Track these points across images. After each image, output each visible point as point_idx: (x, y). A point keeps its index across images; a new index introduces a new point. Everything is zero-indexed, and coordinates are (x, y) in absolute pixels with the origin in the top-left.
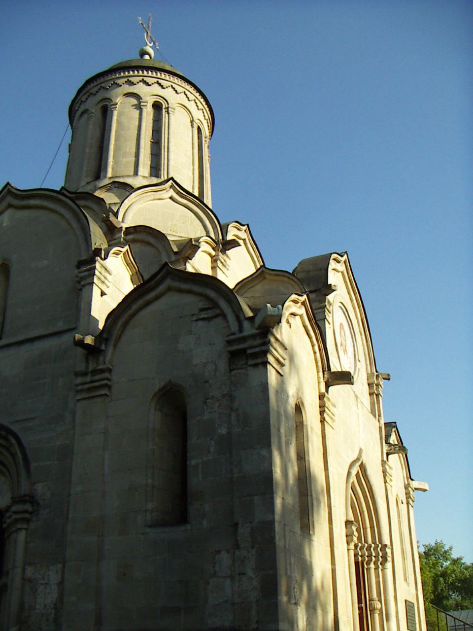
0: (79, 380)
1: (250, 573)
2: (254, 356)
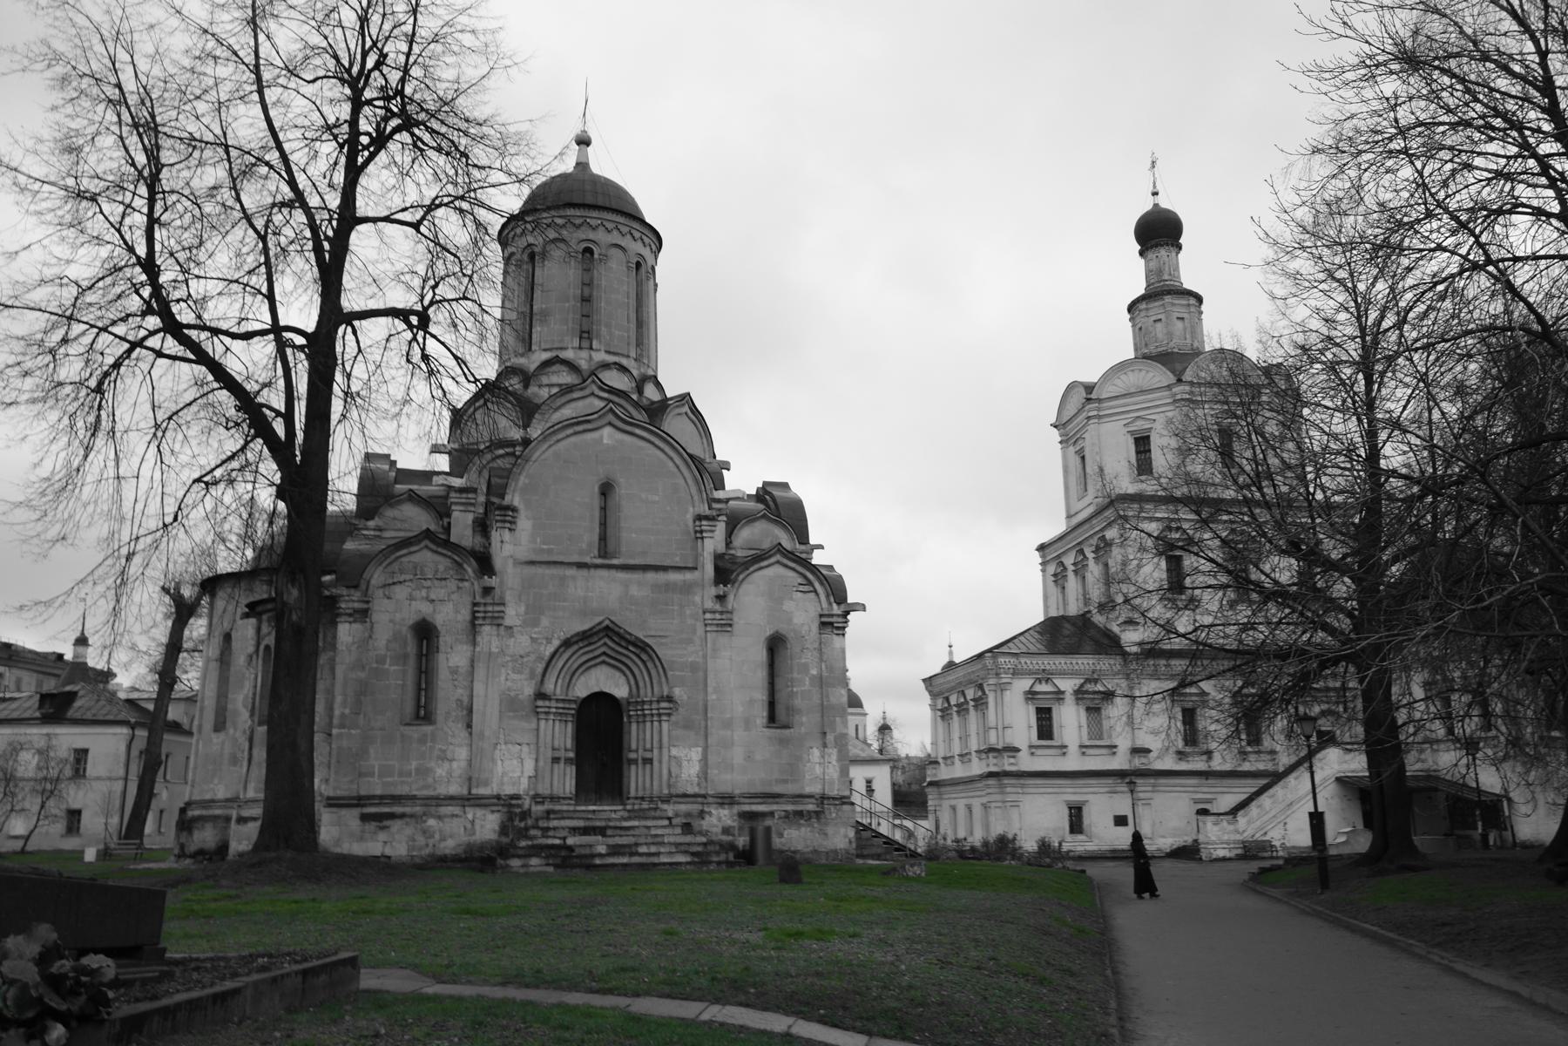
0: (708, 616)
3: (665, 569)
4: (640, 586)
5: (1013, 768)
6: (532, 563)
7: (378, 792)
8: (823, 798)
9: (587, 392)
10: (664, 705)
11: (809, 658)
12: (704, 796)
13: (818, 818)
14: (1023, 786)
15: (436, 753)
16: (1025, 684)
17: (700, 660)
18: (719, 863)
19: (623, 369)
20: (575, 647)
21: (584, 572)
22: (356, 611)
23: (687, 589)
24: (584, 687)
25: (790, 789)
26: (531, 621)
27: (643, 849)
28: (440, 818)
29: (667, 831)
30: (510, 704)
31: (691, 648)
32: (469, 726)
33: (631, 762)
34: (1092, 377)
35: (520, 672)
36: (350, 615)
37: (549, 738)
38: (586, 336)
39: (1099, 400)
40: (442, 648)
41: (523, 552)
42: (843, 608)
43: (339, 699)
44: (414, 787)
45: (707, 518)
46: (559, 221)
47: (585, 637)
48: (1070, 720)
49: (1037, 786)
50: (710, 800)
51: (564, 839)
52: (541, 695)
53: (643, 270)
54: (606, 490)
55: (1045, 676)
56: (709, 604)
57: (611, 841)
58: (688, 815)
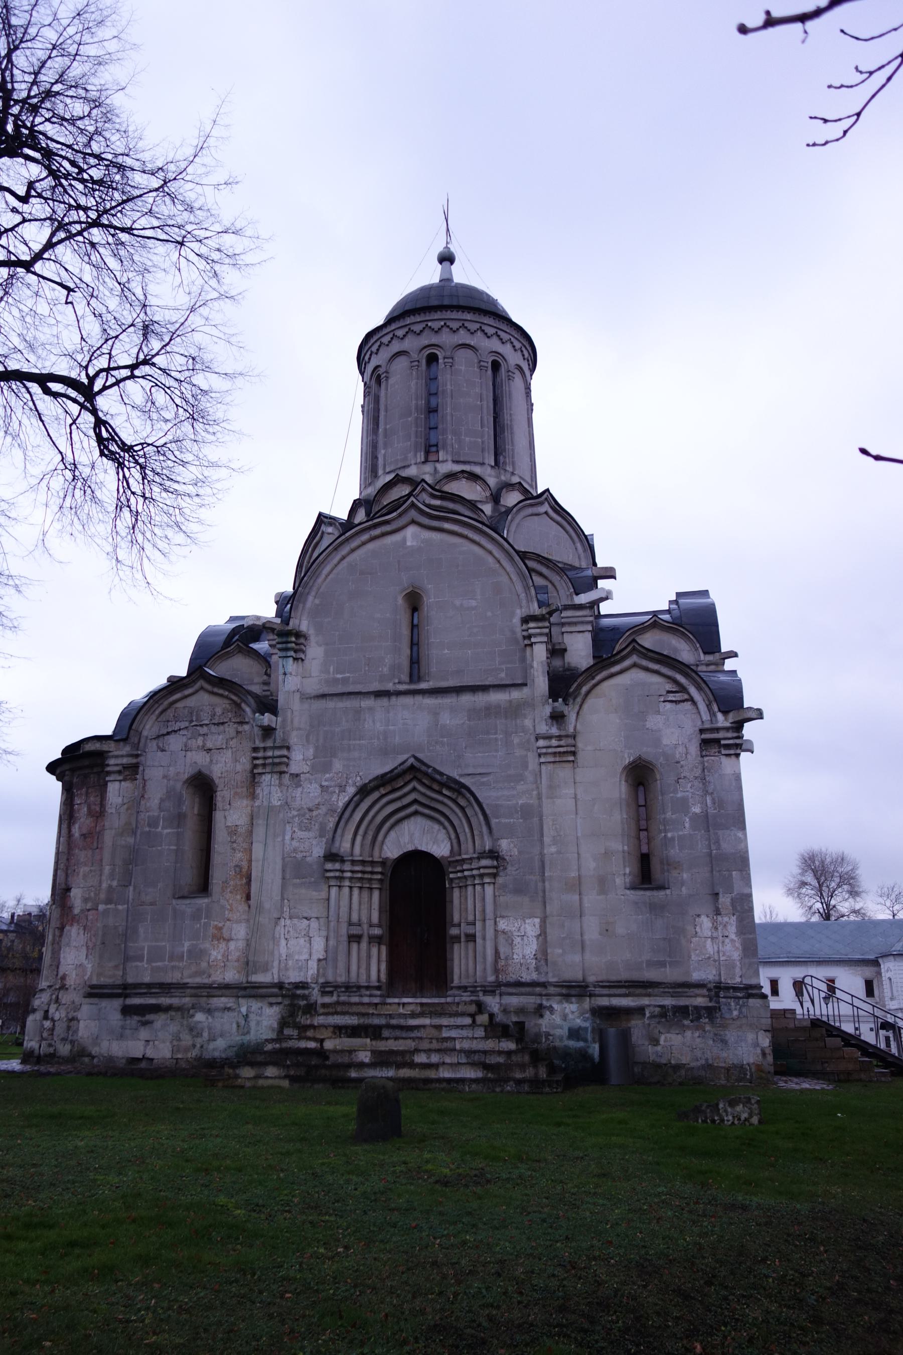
0: (541, 743)
1: (733, 936)
2: (727, 746)
3: (484, 688)
4: (452, 713)
6: (323, 696)
7: (147, 980)
8: (718, 989)
11: (688, 790)
12: (544, 985)
13: (711, 1018)
15: (211, 930)
18: (519, 1082)
19: (474, 477)
20: (376, 795)
21: (384, 701)
22: (126, 767)
23: (514, 711)
24: (394, 846)
25: (670, 975)
26: (321, 765)
27: (421, 1058)
28: (209, 1011)
29: (464, 1033)
30: (294, 869)
31: (521, 787)
32: (248, 897)
35: (308, 829)
36: (119, 772)
37: (344, 910)
38: (430, 450)
41: (313, 686)
42: (732, 717)
44: (186, 973)
46: (400, 333)
47: (385, 781)
51: (322, 1041)
52: (331, 856)
53: (503, 370)
54: (414, 601)
56: (543, 728)
57: (382, 1046)
58: (521, 1011)
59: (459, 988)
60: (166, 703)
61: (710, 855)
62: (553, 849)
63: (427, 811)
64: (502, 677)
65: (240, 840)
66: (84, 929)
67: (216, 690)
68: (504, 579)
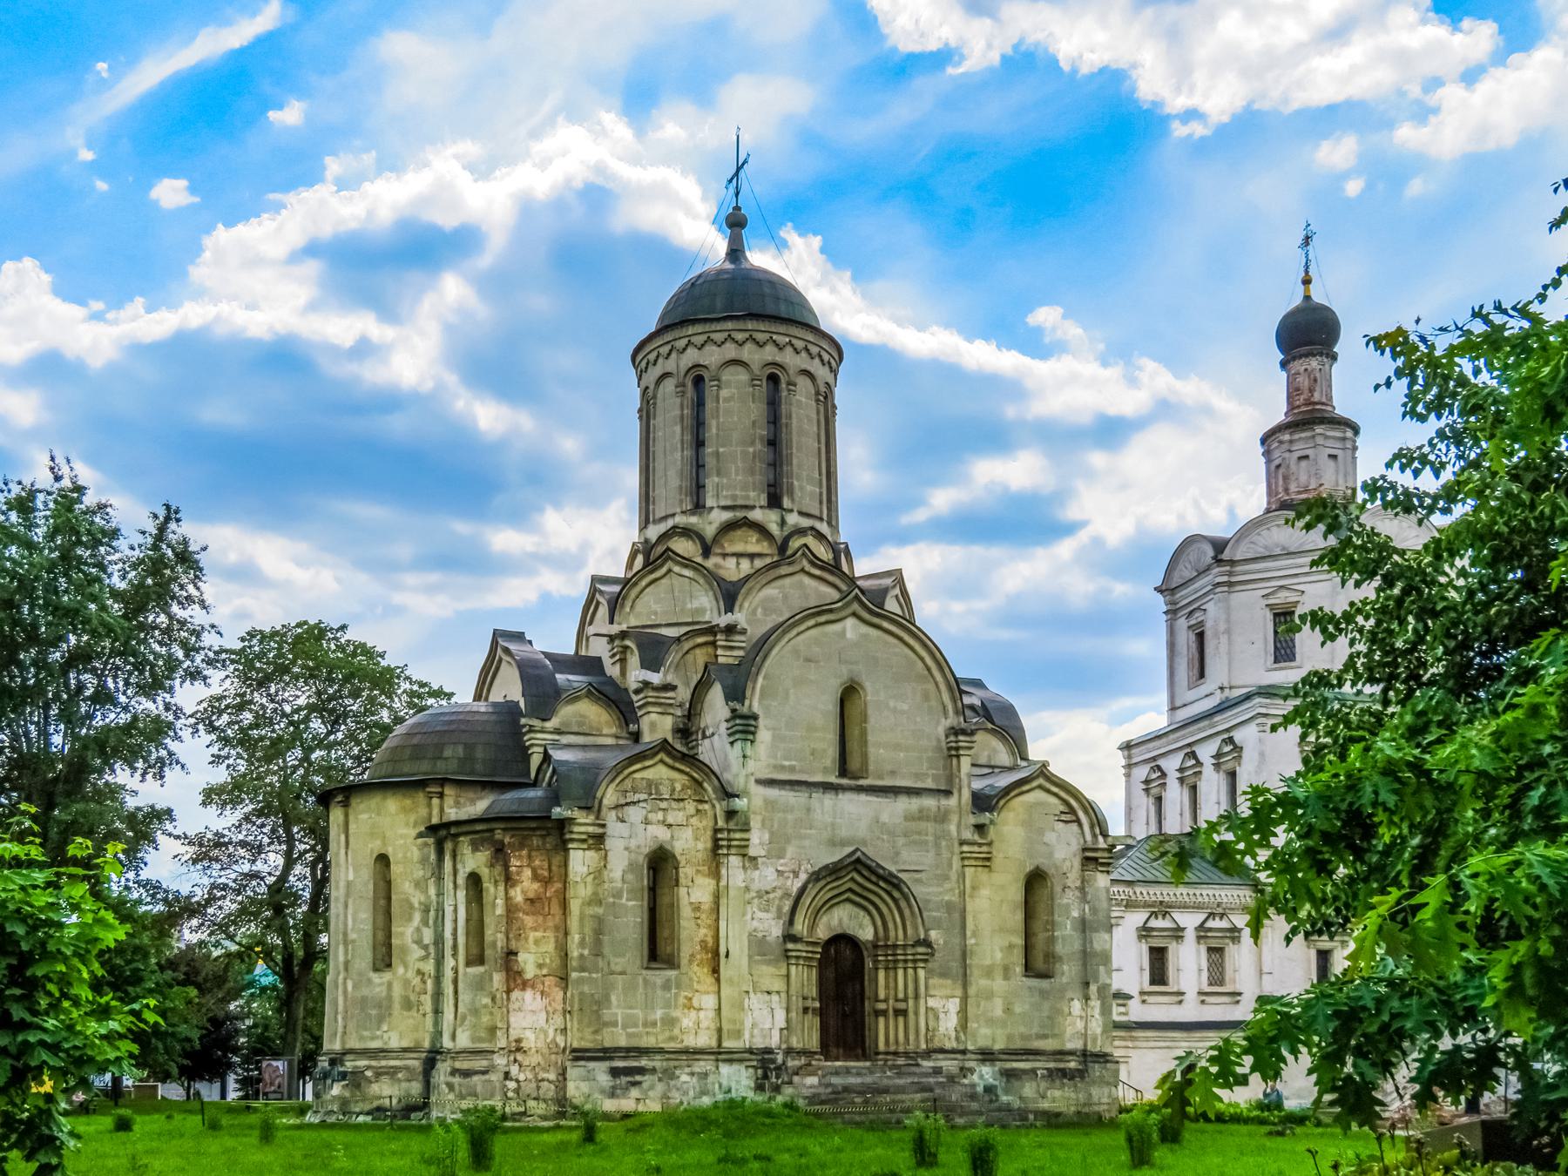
0: (965, 848)
5: (1123, 1018)
9: (796, 568)
10: (921, 950)
12: (964, 1052)
14: (1133, 1039)
16: (1137, 918)
17: (955, 899)
19: (820, 536)
25: (1049, 1045)
30: (758, 946)
31: (947, 886)
32: (715, 971)
33: (878, 1013)
34: (1223, 531)
35: (767, 911)
36: (584, 841)
39: (1232, 563)
40: (682, 881)
43: (575, 938)
45: (963, 732)
47: (832, 872)
48: (1188, 962)
49: (1147, 1039)
50: (969, 1056)
52: (789, 937)
54: (849, 693)
55: (1162, 909)
56: (968, 834)
59: (887, 1053)
60: (626, 772)
61: (1084, 952)
62: (973, 941)
63: (858, 899)
64: (929, 784)
65: (703, 916)
66: (542, 993)
67: (677, 765)
68: (931, 686)
